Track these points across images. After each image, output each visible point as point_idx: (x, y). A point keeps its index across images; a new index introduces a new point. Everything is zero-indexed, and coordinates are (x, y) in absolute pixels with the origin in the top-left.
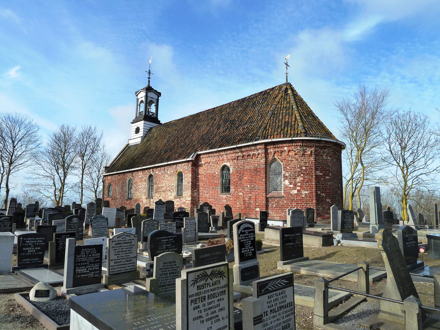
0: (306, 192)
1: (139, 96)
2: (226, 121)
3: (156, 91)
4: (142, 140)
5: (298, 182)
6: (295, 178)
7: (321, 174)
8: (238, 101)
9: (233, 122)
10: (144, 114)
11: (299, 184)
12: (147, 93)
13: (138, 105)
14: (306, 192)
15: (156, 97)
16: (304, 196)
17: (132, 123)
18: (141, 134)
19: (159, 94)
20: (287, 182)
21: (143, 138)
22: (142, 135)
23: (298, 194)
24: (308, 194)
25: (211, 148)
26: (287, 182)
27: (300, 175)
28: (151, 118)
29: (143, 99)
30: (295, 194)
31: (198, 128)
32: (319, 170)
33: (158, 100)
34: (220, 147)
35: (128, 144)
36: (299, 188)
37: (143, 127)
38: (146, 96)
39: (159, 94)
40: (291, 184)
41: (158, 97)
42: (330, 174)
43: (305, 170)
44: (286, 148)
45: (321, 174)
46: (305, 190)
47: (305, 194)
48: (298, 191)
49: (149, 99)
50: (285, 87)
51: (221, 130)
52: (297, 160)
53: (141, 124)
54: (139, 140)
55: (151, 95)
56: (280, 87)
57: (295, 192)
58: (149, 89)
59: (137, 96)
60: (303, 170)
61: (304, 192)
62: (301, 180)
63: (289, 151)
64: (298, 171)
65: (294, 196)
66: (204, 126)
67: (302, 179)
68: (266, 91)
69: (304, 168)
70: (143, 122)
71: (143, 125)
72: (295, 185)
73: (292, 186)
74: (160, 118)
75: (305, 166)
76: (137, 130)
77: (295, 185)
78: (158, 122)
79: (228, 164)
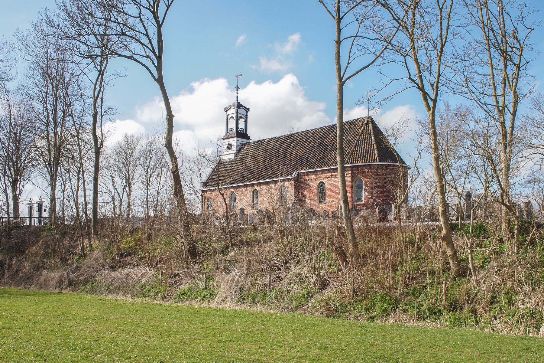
1: (229, 113)
2: (320, 145)
3: (244, 107)
4: (236, 156)
6: (372, 192)
8: (329, 126)
9: (326, 147)
10: (235, 131)
12: (237, 110)
13: (228, 121)
15: (245, 112)
17: (224, 139)
18: (234, 150)
19: (248, 110)
20: (367, 194)
21: (237, 154)
22: (235, 152)
25: (310, 168)
26: (367, 194)
28: (242, 134)
29: (234, 116)
31: (295, 148)
33: (246, 116)
34: (317, 167)
35: (221, 160)
36: (374, 198)
37: (235, 144)
38: (237, 113)
39: (248, 110)
41: (247, 112)
44: (366, 170)
49: (239, 115)
50: (367, 119)
51: (317, 153)
52: (373, 178)
53: (234, 141)
54: (233, 156)
55: (241, 111)
56: (363, 119)
58: (239, 106)
59: (226, 111)
63: (368, 172)
66: (300, 148)
68: (352, 121)
69: (378, 184)
70: (235, 139)
71: (235, 142)
73: (370, 196)
74: (249, 133)
76: (229, 147)
77: (372, 195)
78: (248, 138)
79: (324, 181)
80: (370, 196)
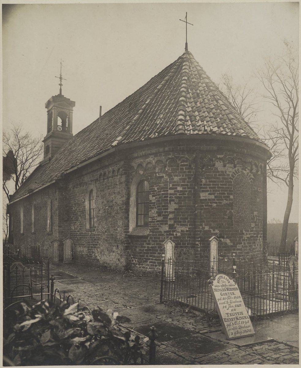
0: (185, 229)
5: (171, 213)
7: (212, 197)
11: (171, 216)
14: (185, 229)
16: (179, 234)
23: (170, 231)
24: (187, 231)
27: (173, 201)
30: (165, 232)
32: (208, 191)
40: (159, 215)
42: (232, 197)
43: (181, 191)
45: (212, 197)
46: (181, 225)
47: (182, 231)
48: (171, 226)
57: (166, 228)
60: (178, 191)
61: (179, 229)
62: (175, 209)
64: (170, 194)
65: (163, 235)
67: (176, 206)
69: (179, 188)
72: (166, 217)
73: (160, 218)
75: (182, 185)
80: (160, 218)
